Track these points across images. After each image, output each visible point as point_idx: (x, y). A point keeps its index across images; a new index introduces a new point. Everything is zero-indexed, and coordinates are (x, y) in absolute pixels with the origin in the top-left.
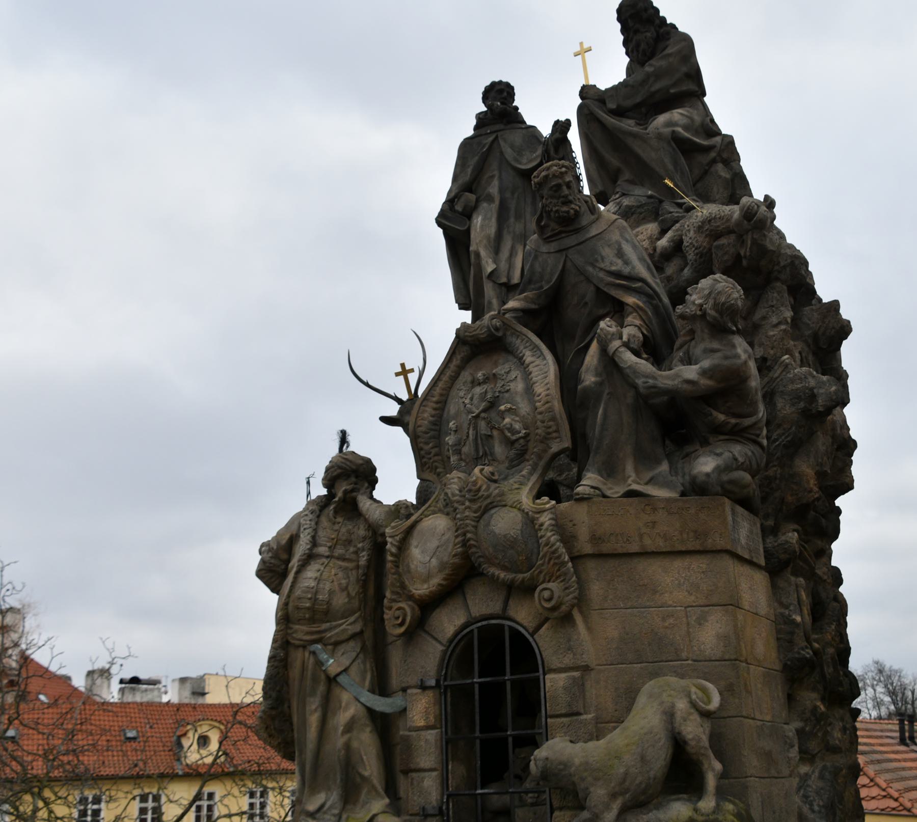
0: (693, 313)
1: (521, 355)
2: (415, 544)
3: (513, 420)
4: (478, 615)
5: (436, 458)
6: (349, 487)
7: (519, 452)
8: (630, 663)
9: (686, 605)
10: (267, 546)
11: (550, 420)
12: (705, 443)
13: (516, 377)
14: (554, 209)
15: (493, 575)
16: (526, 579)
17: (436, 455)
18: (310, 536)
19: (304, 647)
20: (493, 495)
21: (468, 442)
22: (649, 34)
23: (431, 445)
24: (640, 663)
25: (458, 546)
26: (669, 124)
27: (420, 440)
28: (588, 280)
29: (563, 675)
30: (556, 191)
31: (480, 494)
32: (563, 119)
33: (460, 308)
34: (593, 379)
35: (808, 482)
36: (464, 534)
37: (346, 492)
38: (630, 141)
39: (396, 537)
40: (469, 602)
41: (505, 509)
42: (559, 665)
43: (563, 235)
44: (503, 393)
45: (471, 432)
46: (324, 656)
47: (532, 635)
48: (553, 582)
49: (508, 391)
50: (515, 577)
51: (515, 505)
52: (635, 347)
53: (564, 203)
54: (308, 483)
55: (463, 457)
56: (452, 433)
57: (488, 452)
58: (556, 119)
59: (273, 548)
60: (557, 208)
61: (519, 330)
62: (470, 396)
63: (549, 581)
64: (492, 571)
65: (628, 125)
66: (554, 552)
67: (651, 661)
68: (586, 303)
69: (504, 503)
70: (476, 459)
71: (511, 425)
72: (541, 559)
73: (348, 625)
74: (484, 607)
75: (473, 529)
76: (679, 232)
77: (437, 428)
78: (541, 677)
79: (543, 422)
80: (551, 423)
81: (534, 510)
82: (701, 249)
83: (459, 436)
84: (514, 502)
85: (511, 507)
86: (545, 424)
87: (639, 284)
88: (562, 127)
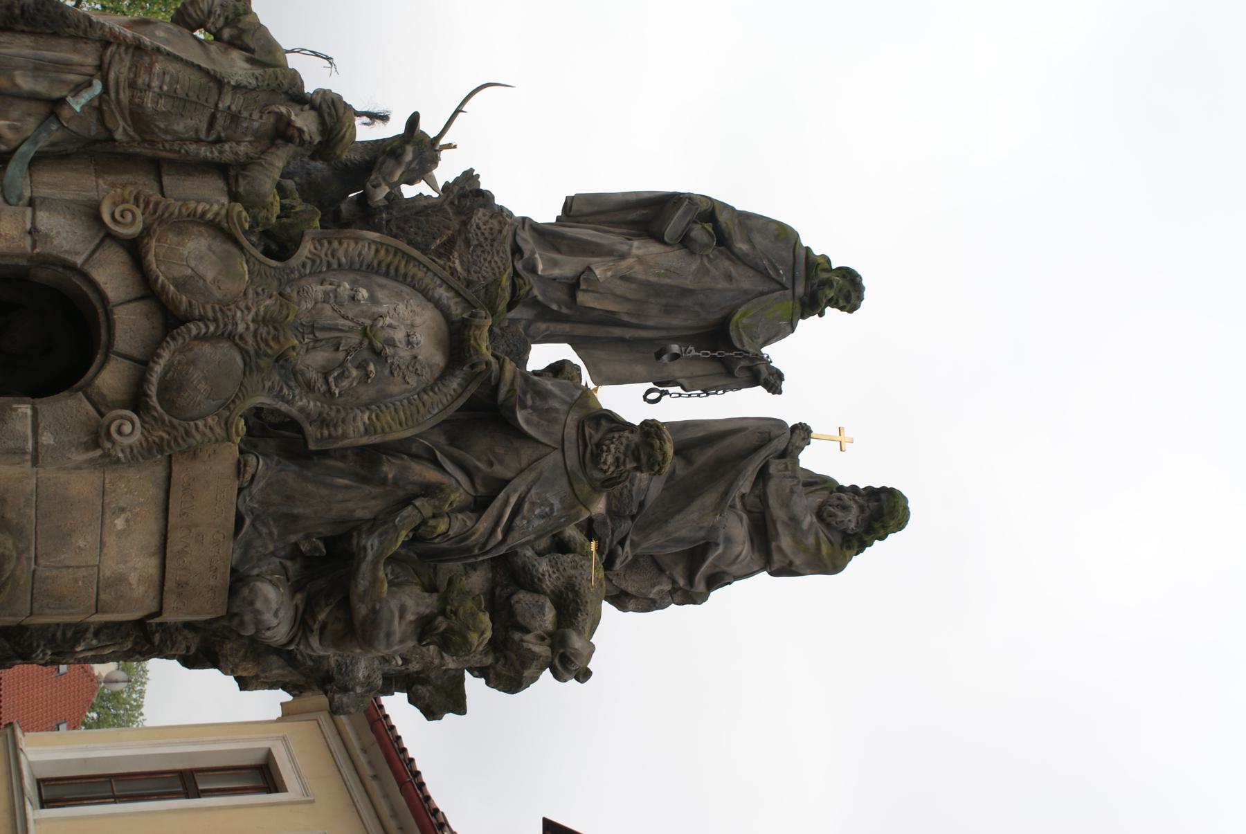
0: (450, 601)
1: (436, 389)
2: (212, 246)
3: (354, 379)
4: (115, 317)
5: (325, 264)
6: (307, 137)
7: (312, 384)
8: (36, 506)
9: (101, 566)
10: (245, 10)
12: (296, 588)
13: (408, 383)
14: (612, 447)
15: (159, 356)
16: (148, 400)
17: (329, 265)
18: (248, 84)
19: (99, 68)
20: (259, 361)
21: (336, 315)
22: (852, 525)
24: (36, 516)
25: (202, 311)
26: (728, 540)
27: (352, 245)
30: (633, 453)
31: (262, 345)
32: (784, 386)
33: (567, 198)
34: (390, 476)
35: (245, 670)
36: (215, 320)
37: (300, 131)
38: (721, 488)
39: (225, 220)
40: (133, 305)
42: (42, 425)
43: (581, 448)
44: (391, 368)
46: (85, 97)
48: (142, 433)
49: (392, 373)
50: (153, 385)
51: (243, 388)
52: (420, 531)
53: (617, 459)
54: (328, 58)
55: (319, 306)
56: (353, 292)
57: (317, 345)
58: (785, 377)
60: (613, 450)
61: (469, 387)
62: (394, 323)
63: (142, 426)
64: (164, 354)
65: (745, 485)
67: (38, 527)
68: (491, 464)
69: (247, 373)
70: (313, 326)
71: (348, 378)
72: (170, 422)
73: (124, 129)
74: (125, 327)
75: (219, 333)
76: (579, 550)
77: (364, 268)
79: (343, 421)
80: (340, 431)
81: (231, 420)
82: (548, 583)
83: (346, 303)
84: (245, 388)
85: (242, 383)
86: (340, 423)
87: (499, 536)
88: (773, 381)
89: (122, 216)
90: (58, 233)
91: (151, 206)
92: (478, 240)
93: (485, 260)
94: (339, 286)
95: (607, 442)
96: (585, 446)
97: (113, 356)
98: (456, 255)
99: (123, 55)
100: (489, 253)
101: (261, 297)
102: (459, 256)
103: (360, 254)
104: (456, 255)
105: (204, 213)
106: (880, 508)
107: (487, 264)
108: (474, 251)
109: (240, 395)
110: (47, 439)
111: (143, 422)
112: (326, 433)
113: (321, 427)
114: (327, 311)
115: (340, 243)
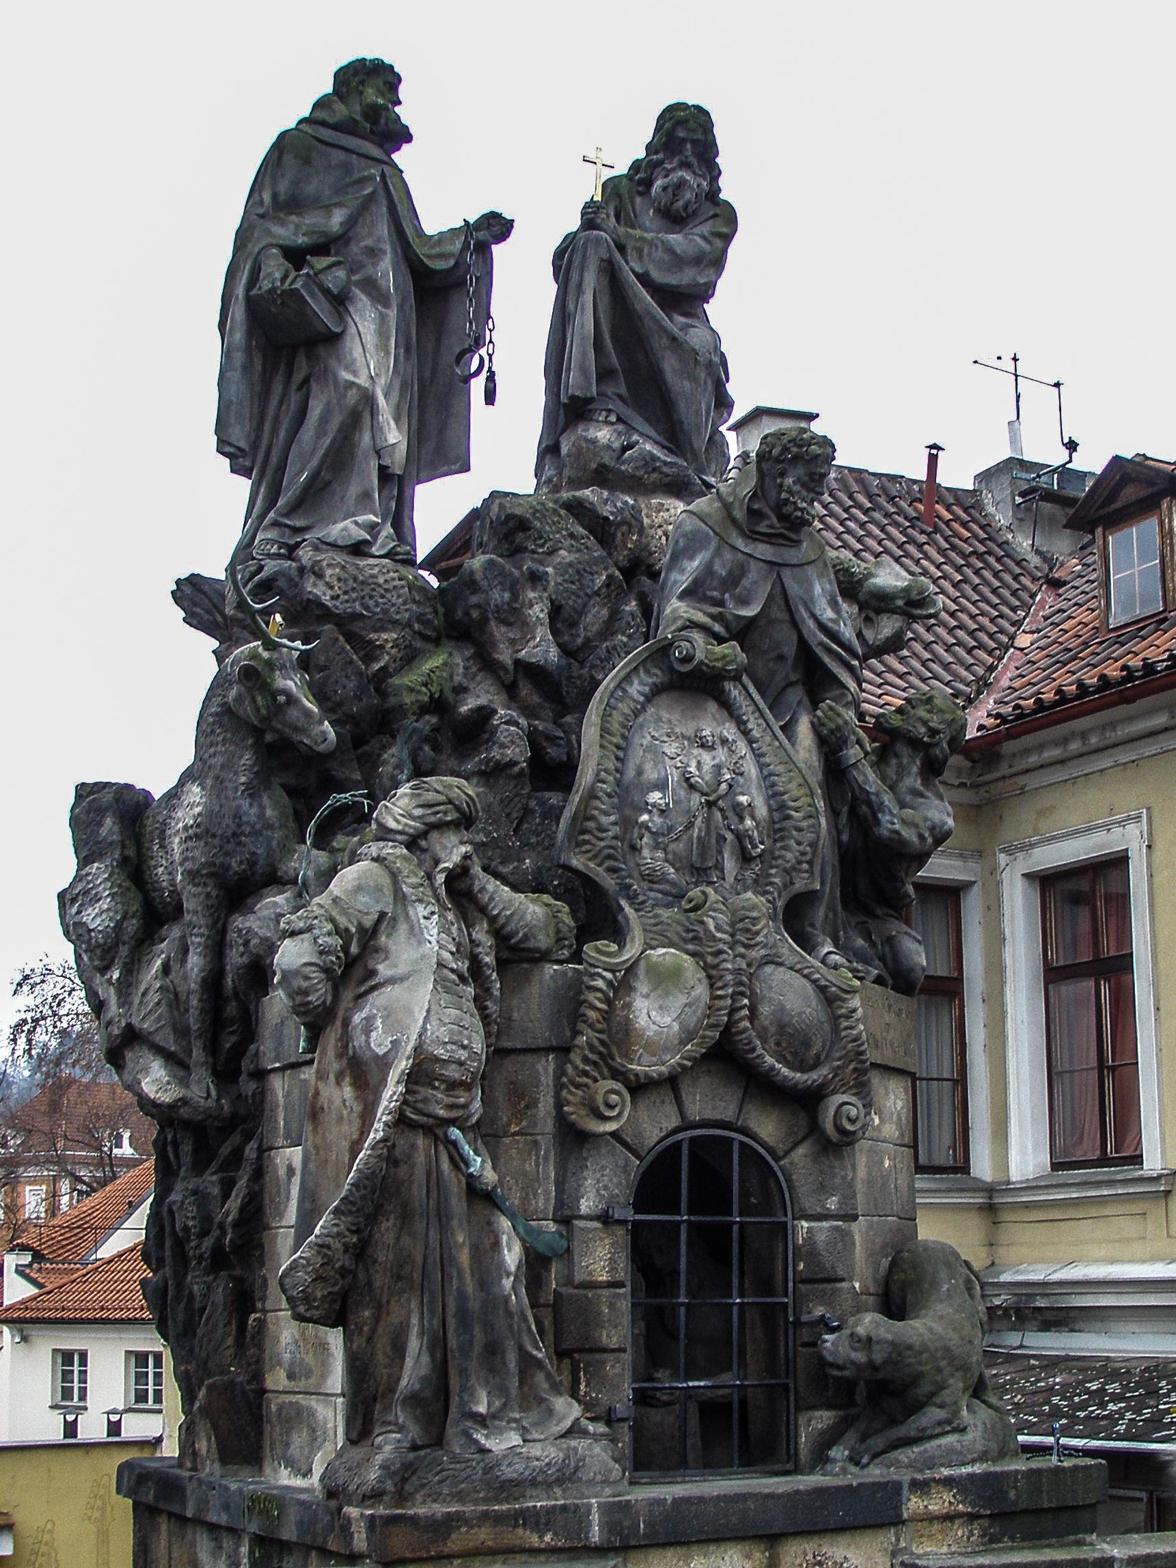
5: (614, 842)
11: (810, 845)
19: (428, 1130)
23: (612, 818)
28: (794, 623)
29: (825, 1224)
30: (813, 480)
41: (781, 969)
43: (781, 541)
45: (699, 822)
47: (777, 1159)
55: (670, 857)
59: (347, 930)
66: (862, 1053)
68: (781, 658)
78: (789, 1224)
85: (791, 968)
89: (612, 1107)
90: (606, 1188)
91: (587, 1068)
92: (354, 601)
93: (382, 597)
94: (648, 828)
95: (790, 508)
96: (781, 536)
97: (739, 1123)
98: (373, 636)
99: (419, 1097)
100: (374, 590)
101: (702, 934)
102: (376, 631)
103: (609, 796)
104: (373, 636)
105: (609, 1002)
106: (695, 142)
107: (388, 595)
108: (367, 608)
109: (806, 972)
110: (832, 1204)
111: (834, 1092)
112: (805, 866)
113: (800, 871)
114: (680, 847)
115: (592, 818)
